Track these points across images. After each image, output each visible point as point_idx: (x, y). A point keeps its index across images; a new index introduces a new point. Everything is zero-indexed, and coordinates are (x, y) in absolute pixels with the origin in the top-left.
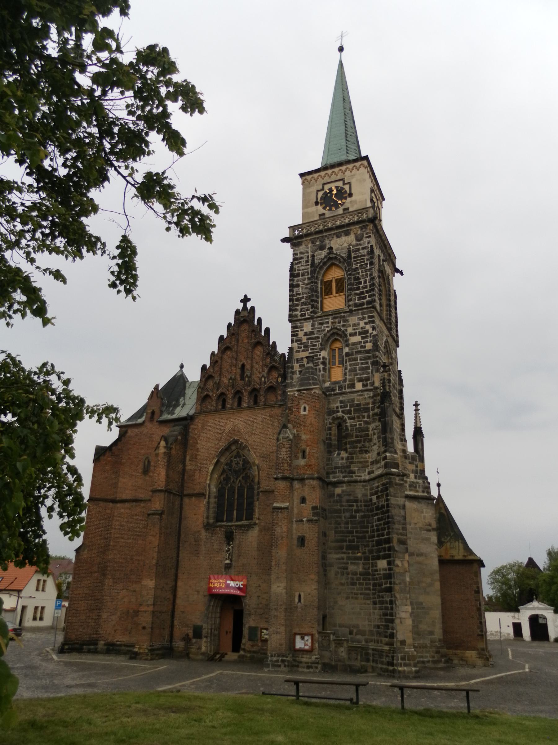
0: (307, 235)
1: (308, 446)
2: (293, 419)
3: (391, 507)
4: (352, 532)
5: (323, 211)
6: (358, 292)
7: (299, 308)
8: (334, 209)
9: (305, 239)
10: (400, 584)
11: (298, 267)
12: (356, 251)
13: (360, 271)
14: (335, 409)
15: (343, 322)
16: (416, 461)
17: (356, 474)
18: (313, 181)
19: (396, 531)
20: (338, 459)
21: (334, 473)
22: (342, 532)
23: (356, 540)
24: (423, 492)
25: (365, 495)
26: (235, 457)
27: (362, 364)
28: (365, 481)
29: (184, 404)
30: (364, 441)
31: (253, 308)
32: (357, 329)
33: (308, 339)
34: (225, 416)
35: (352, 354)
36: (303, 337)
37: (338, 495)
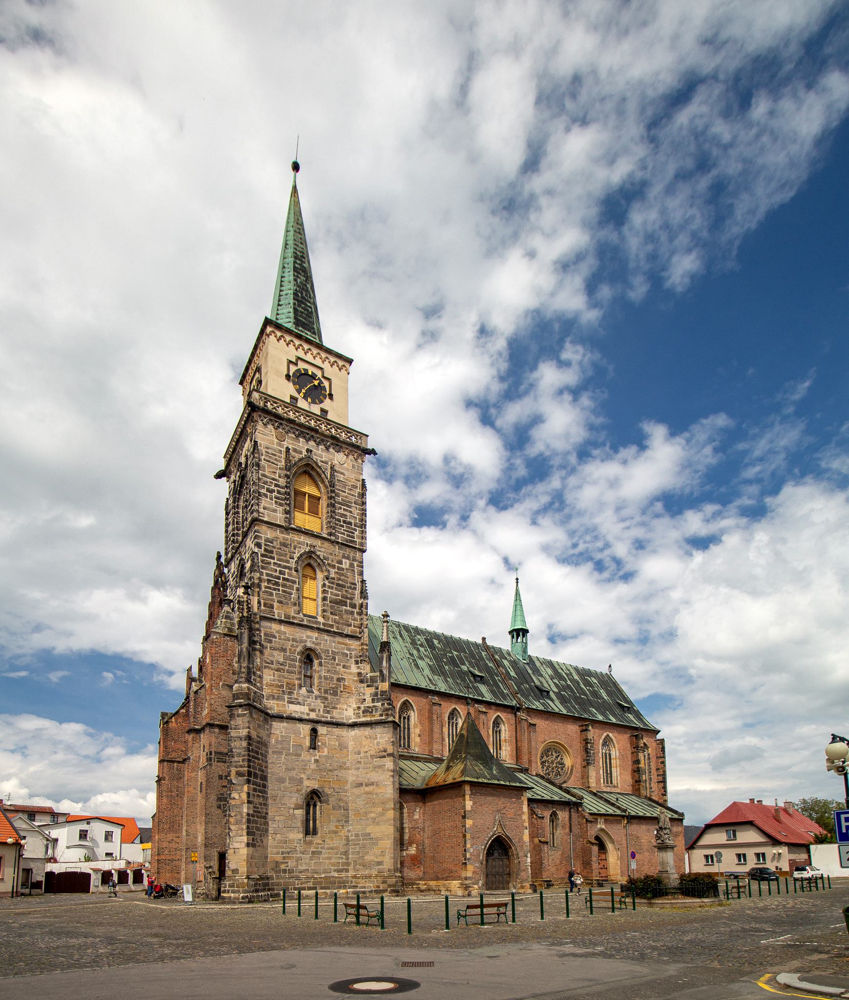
24: (381, 715)
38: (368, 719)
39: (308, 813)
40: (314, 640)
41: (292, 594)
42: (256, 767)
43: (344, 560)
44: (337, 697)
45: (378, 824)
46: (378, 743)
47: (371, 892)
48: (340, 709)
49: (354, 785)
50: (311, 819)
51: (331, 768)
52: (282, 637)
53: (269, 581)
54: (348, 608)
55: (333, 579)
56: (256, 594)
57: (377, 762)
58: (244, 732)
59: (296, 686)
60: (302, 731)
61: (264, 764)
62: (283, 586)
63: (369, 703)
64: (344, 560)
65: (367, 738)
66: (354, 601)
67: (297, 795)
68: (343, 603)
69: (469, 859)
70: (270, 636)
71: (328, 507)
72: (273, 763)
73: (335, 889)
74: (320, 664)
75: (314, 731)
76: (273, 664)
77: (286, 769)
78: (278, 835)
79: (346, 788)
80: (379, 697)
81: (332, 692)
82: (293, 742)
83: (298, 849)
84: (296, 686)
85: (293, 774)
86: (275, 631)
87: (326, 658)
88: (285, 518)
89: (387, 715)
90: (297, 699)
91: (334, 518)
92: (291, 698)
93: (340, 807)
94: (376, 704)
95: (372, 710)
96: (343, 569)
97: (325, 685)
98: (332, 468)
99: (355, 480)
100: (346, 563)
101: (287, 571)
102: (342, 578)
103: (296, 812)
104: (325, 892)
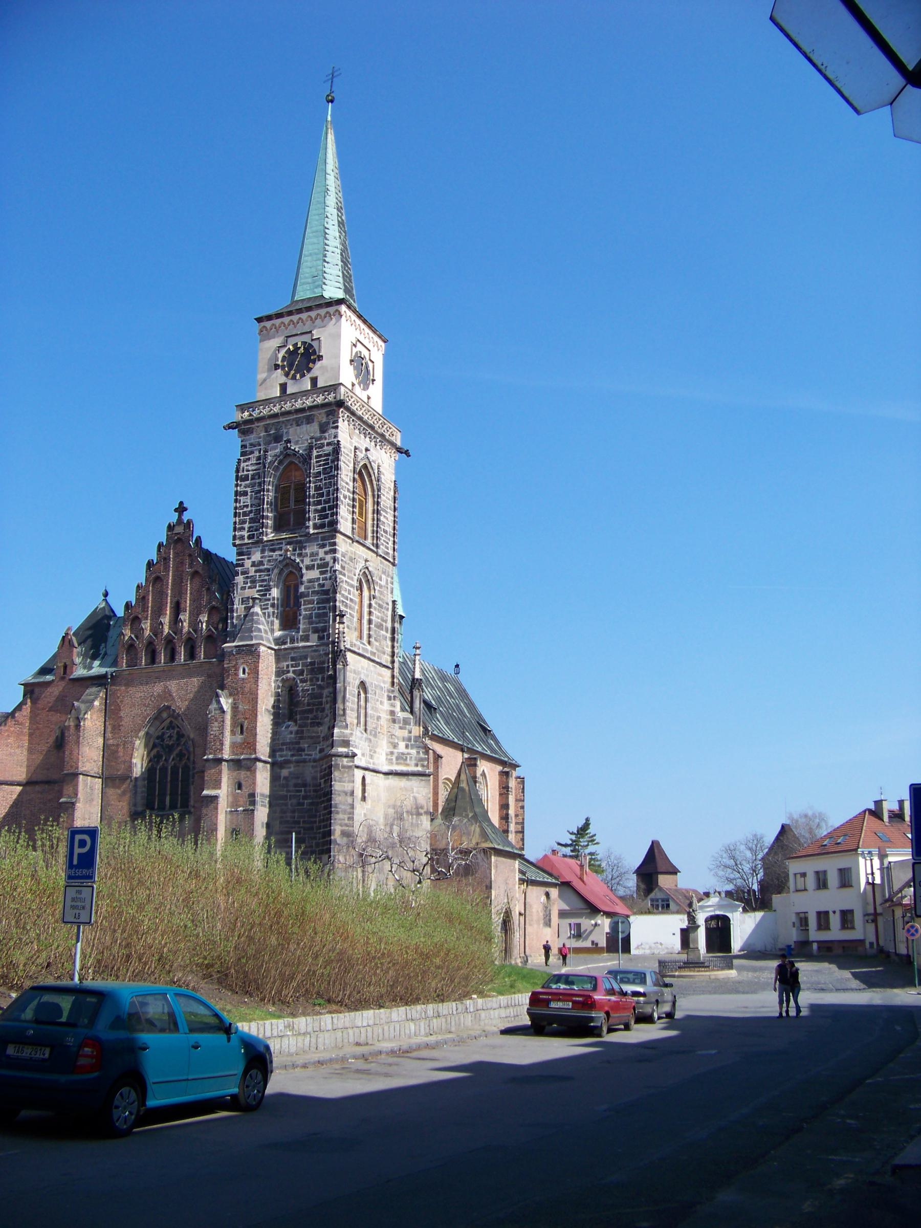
0: (259, 419)
1: (247, 718)
2: (230, 684)
3: (335, 794)
4: (299, 823)
5: (283, 379)
6: (319, 507)
7: (247, 526)
8: (298, 376)
9: (256, 424)
11: (247, 466)
12: (320, 448)
13: (322, 476)
14: (285, 669)
15: (299, 550)
16: (410, 724)
17: (306, 752)
18: (274, 330)
19: (339, 822)
20: (286, 733)
21: (281, 750)
22: (287, 822)
23: (302, 832)
24: (417, 765)
25: (314, 778)
26: (168, 728)
27: (319, 608)
28: (315, 761)
29: (106, 654)
30: (317, 710)
31: (189, 522)
32: (315, 560)
33: (256, 571)
34: (153, 674)
35: (308, 595)
36: (250, 568)
37: (285, 778)
38: (404, 768)
75: (364, 778)
80: (412, 742)
89: (423, 766)
94: (410, 751)
95: (406, 757)
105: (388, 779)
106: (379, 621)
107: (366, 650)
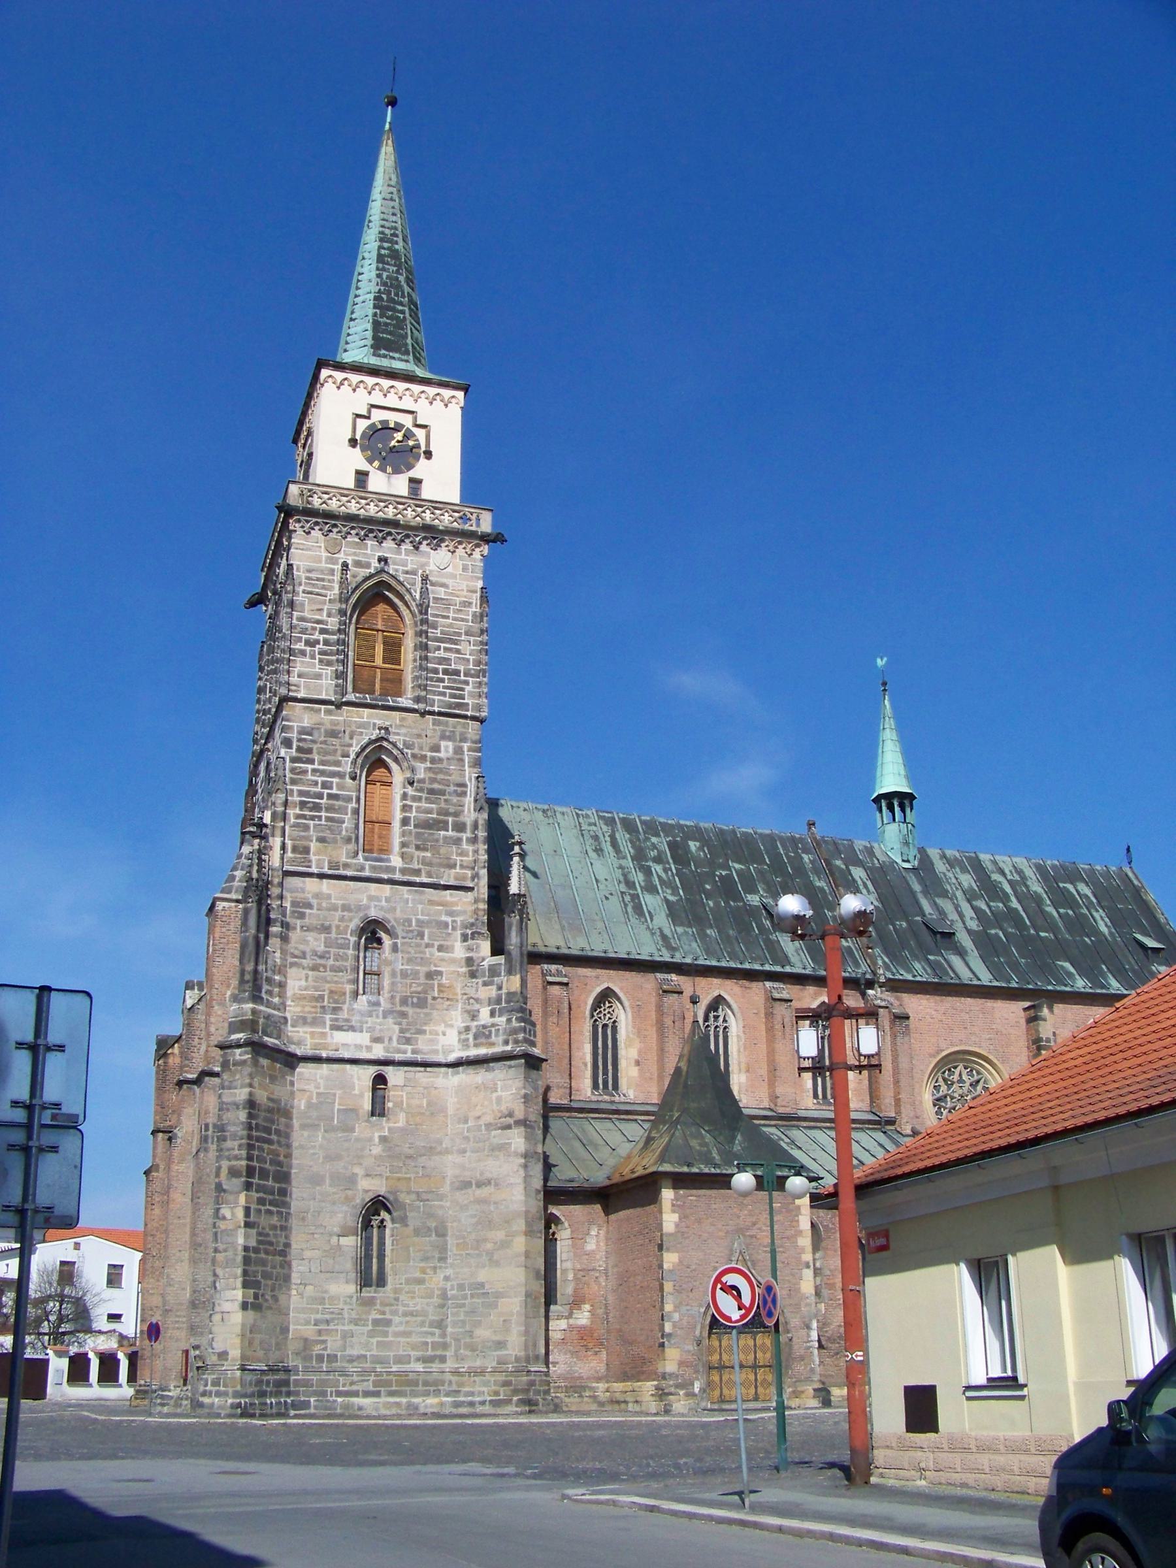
10: (225, 1251)
38: (482, 1051)
39: (368, 1242)
40: (384, 903)
41: (344, 822)
42: (265, 1158)
43: (443, 744)
44: (425, 1011)
45: (497, 1264)
46: (499, 1099)
47: (483, 1403)
48: (431, 1033)
49: (457, 1184)
50: (375, 1254)
51: (411, 1152)
52: (324, 905)
53: (303, 805)
54: (450, 833)
55: (420, 781)
56: (278, 832)
57: (497, 1136)
58: (242, 1094)
59: (348, 996)
60: (356, 1082)
61: (282, 1151)
62: (328, 810)
63: (485, 1012)
64: (443, 744)
65: (480, 1091)
66: (462, 819)
67: (345, 1208)
68: (442, 825)
69: (670, 1335)
70: (302, 906)
71: (415, 650)
72: (301, 1147)
73: (416, 1396)
74: (395, 948)
75: (380, 1080)
76: (305, 958)
77: (325, 1158)
78: (310, 1288)
79: (442, 1190)
81: (415, 1000)
82: (339, 1104)
83: (346, 1316)
84: (348, 996)
85: (339, 1166)
86: (310, 896)
87: (404, 935)
88: (336, 686)
90: (347, 1020)
91: (427, 669)
92: (336, 1020)
93: (429, 1229)
94: (497, 1020)
95: (490, 1032)
96: (440, 760)
97: (402, 990)
98: (425, 579)
99: (469, 591)
100: (447, 747)
101: (335, 780)
102: (440, 776)
103: (344, 1241)
104: (397, 1403)
105: (458, 1073)
106: (435, 816)
107: (392, 870)
